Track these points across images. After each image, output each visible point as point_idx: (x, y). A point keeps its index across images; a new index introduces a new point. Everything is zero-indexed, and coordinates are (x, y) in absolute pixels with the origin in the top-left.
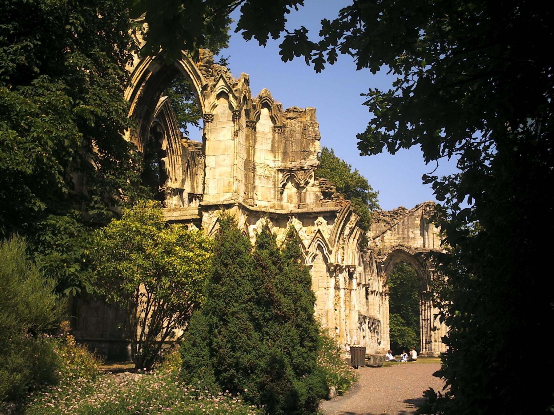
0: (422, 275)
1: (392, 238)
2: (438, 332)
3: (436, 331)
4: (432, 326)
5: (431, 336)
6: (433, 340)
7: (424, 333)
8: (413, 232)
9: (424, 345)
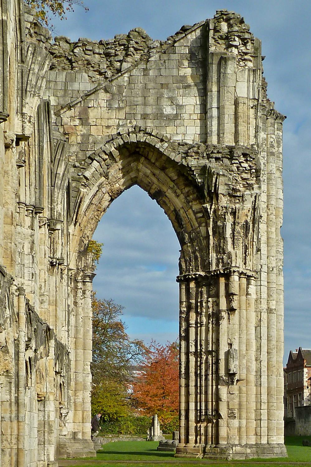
0: (197, 225)
1: (113, 114)
2: (240, 390)
3: (235, 388)
4: (222, 372)
5: (218, 399)
6: (223, 411)
7: (192, 390)
8: (172, 99)
9: (192, 424)
